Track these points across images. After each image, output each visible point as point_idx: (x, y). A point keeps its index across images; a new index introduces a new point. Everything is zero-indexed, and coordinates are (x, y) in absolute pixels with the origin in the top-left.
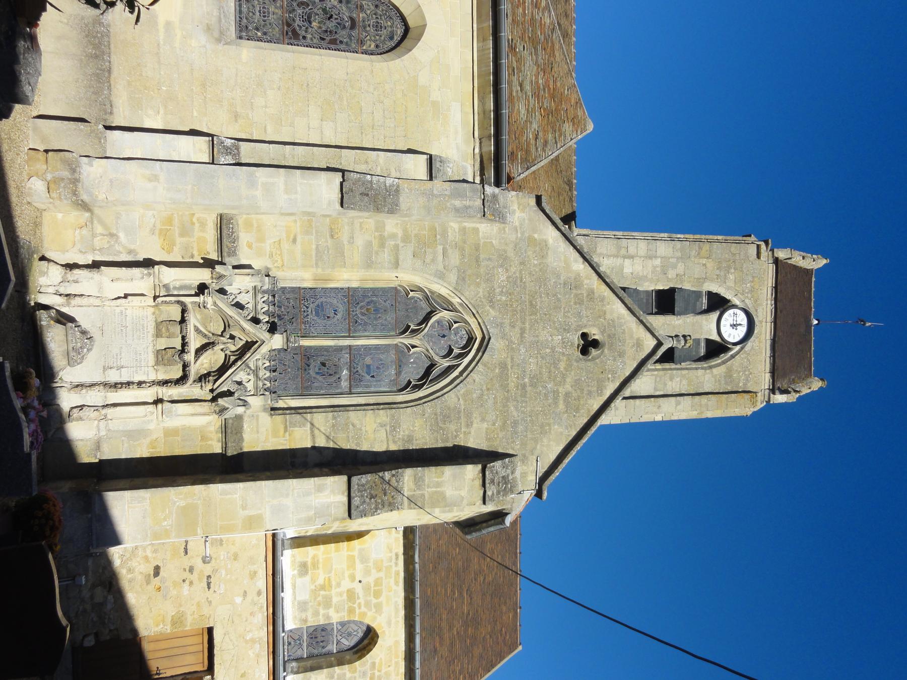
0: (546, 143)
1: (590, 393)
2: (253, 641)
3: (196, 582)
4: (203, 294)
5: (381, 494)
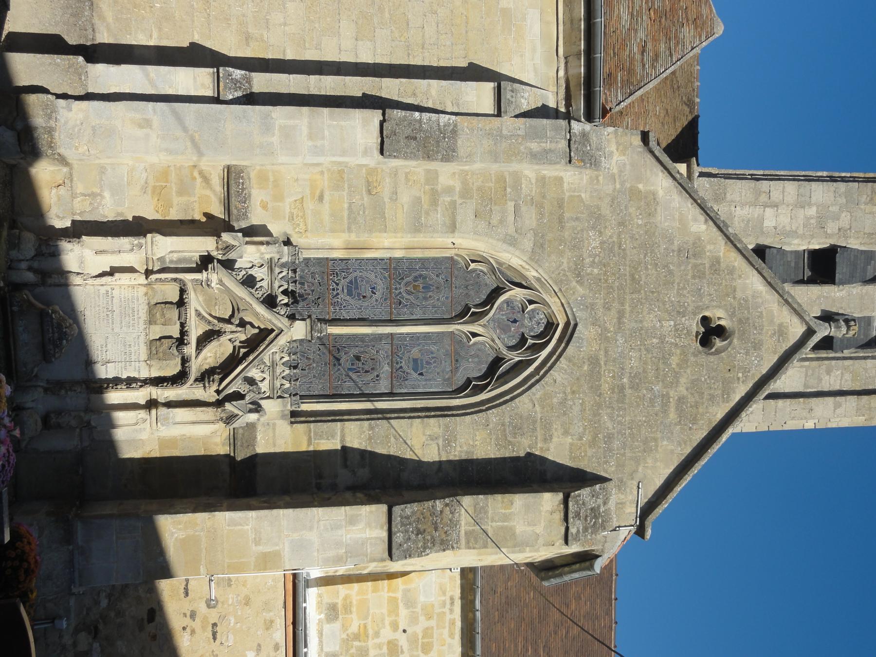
0: (656, 57)
1: (712, 398)
3: (198, 631)
4: (207, 270)
5: (431, 529)
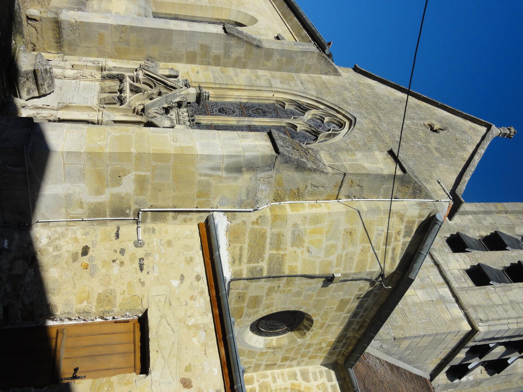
2: (196, 327)
